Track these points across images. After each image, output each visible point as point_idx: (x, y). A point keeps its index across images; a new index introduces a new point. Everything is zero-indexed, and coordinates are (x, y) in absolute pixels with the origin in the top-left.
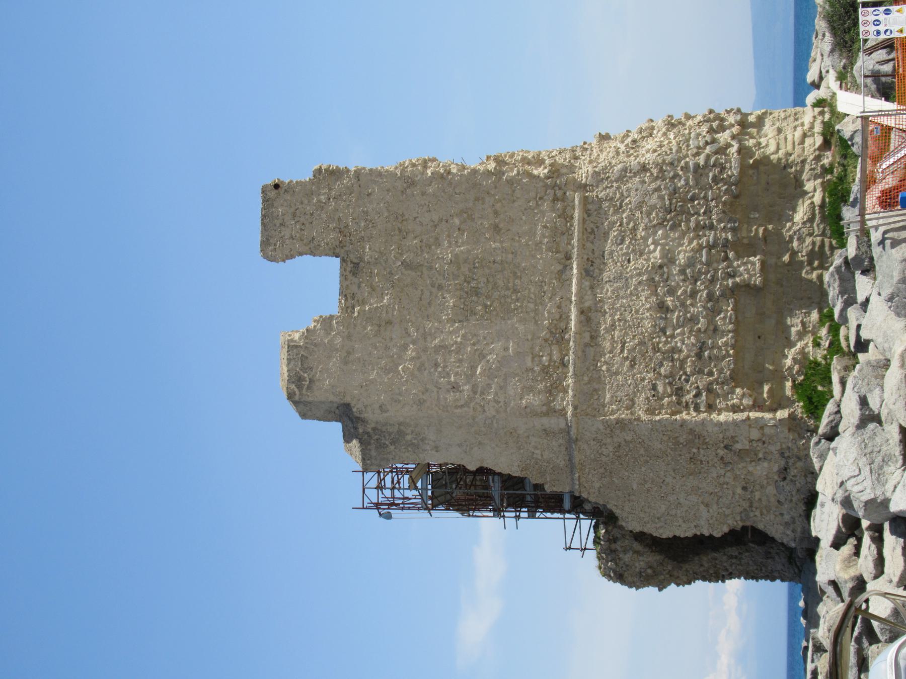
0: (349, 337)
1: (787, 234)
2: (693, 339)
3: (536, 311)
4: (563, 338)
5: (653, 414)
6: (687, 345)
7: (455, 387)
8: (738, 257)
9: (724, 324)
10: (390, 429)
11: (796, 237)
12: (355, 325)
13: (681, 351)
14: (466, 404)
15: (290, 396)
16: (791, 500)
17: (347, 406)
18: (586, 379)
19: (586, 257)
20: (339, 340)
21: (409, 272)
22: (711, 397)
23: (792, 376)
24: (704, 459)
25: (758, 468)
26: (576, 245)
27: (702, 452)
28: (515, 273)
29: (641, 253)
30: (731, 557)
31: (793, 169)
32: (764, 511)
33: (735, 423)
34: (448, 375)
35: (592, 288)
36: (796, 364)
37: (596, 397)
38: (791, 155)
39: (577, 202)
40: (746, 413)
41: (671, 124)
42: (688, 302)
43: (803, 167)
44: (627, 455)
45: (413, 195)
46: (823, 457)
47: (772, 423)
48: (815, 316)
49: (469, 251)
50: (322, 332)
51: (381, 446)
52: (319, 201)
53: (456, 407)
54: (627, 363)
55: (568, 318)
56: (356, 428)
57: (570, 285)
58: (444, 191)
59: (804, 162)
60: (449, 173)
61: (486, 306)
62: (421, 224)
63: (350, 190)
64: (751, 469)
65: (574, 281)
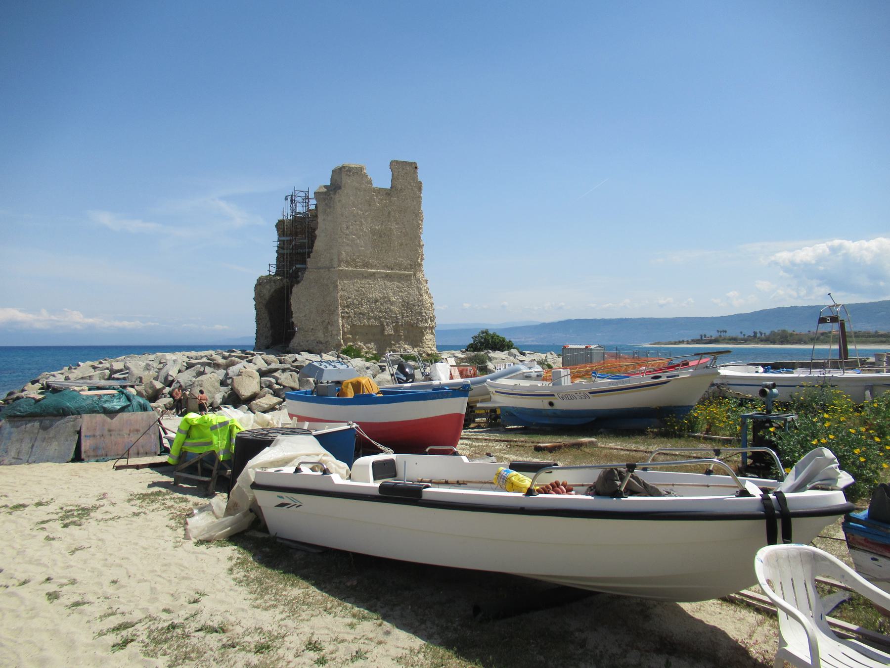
7: (348, 228)
15: (343, 167)
17: (340, 188)
41: (432, 304)
46: (332, 355)
48: (375, 352)
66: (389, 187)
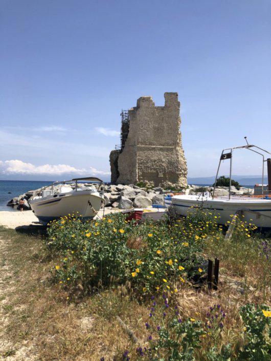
7: (142, 127)
15: (141, 98)
29: (164, 157)
33: (136, 172)
41: (185, 163)
46: (131, 186)
48: (153, 185)
51: (133, 114)
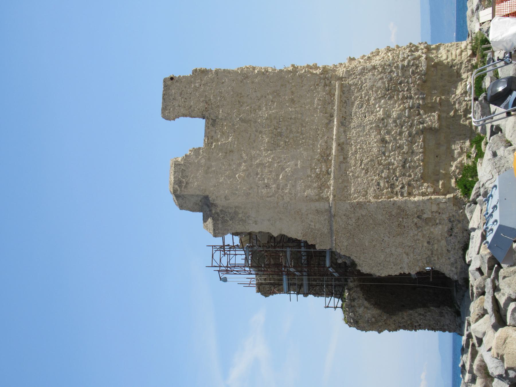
0: (209, 159)
1: (452, 101)
2: (400, 158)
3: (313, 145)
4: (328, 159)
5: (378, 198)
6: (397, 161)
7: (267, 186)
8: (425, 113)
9: (418, 149)
10: (230, 211)
11: (457, 102)
12: (213, 153)
13: (393, 164)
14: (273, 195)
15: (175, 192)
16: (455, 248)
17: (206, 198)
18: (340, 181)
19: (341, 115)
20: (203, 161)
21: (244, 124)
22: (410, 188)
23: (455, 176)
24: (406, 225)
25: (436, 229)
26: (336, 109)
27: (405, 220)
28: (302, 124)
30: (420, 314)
31: (456, 67)
32: (440, 257)
33: (423, 201)
34: (264, 179)
35: (345, 132)
36: (457, 169)
37: (346, 190)
38: (454, 60)
39: (337, 86)
40: (429, 197)
41: (389, 49)
42: (398, 138)
43: (461, 66)
44: (362, 224)
45: (247, 83)
46: (472, 212)
47: (444, 200)
48: (468, 143)
49: (277, 113)
50: (194, 156)
52: (195, 86)
53: (268, 197)
54: (364, 171)
55: (331, 148)
56: (211, 211)
57: (333, 131)
58: (264, 81)
59: (461, 63)
60: (267, 71)
61: (285, 142)
62: (251, 98)
63: (212, 81)
64: (432, 230)
65: (335, 128)
66: (202, 122)
